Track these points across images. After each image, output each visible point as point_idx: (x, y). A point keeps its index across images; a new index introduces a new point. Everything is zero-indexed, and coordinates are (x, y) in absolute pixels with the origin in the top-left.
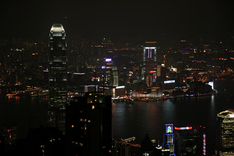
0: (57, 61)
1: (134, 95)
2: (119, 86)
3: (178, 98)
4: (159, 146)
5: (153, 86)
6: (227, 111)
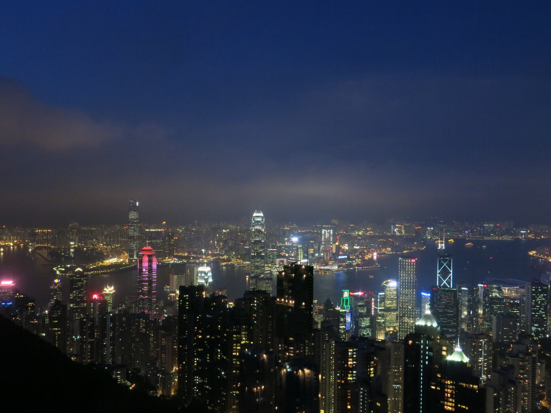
0: (257, 239)
4: (338, 307)
5: (329, 260)
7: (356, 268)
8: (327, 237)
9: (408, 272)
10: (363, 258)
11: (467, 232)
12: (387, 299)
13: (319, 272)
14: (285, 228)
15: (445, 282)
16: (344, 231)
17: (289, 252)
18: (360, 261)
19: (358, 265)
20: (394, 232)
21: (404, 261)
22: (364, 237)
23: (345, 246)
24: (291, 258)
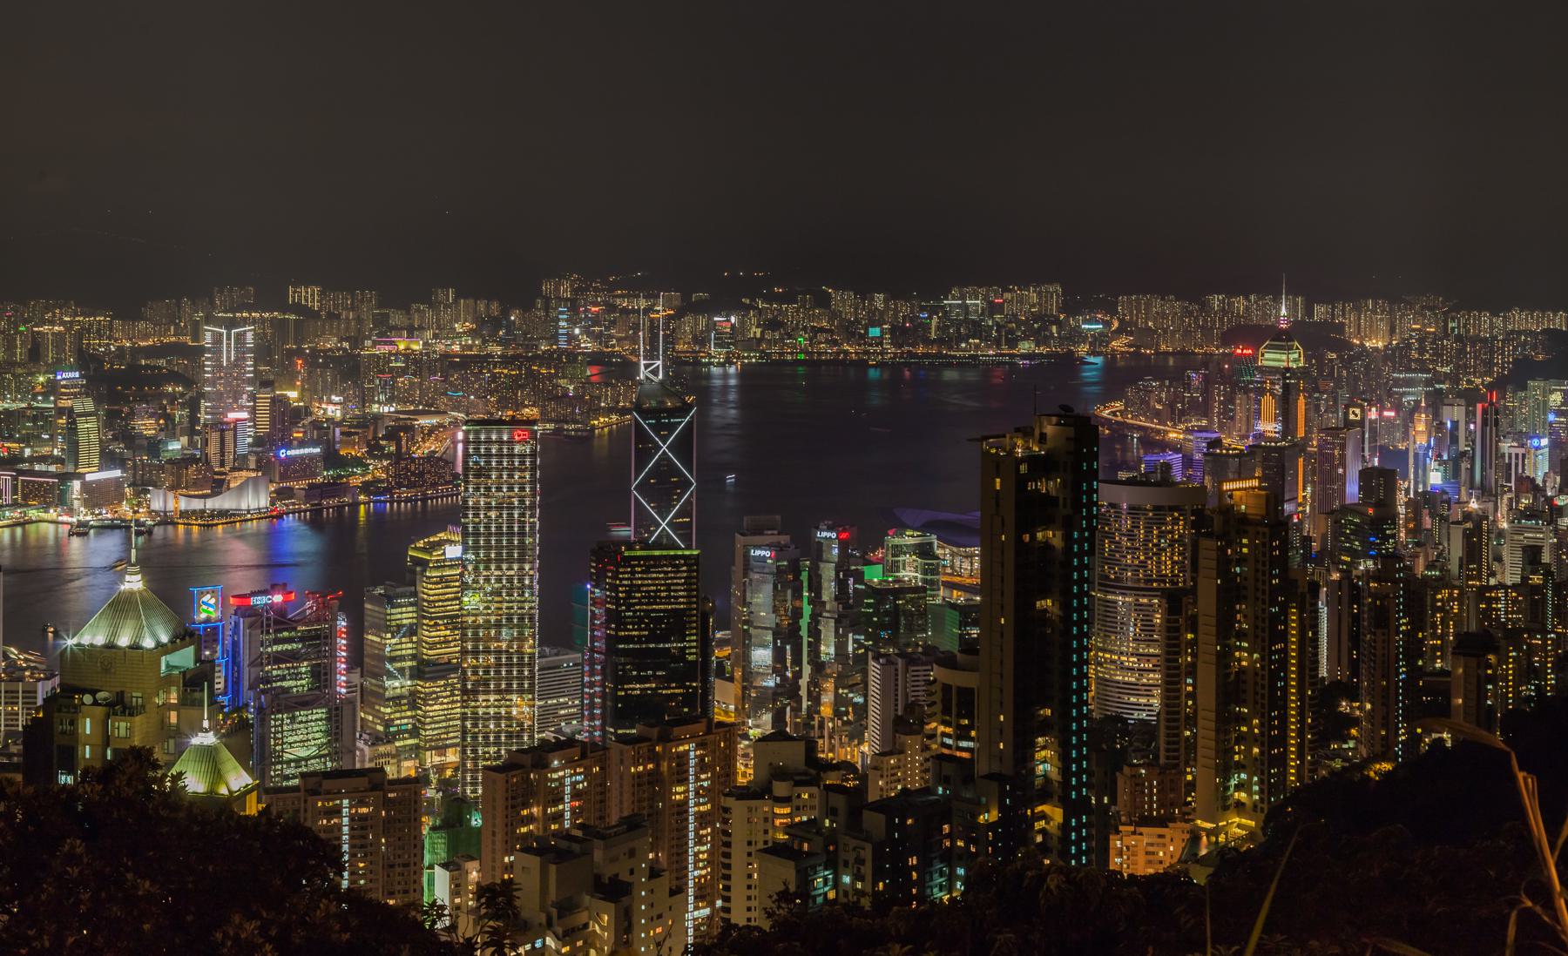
1: (157, 505)
2: (100, 470)
3: (328, 509)
5: (234, 469)
6: (442, 535)
7: (362, 497)
8: (229, 358)
9: (499, 489)
10: (398, 457)
11: (875, 332)
12: (431, 619)
13: (175, 524)
14: (43, 323)
15: (664, 525)
16: (341, 340)
17: (39, 437)
18: (386, 470)
19: (366, 488)
20: (571, 338)
21: (483, 437)
22: (417, 364)
23: (330, 402)
24: (37, 467)
